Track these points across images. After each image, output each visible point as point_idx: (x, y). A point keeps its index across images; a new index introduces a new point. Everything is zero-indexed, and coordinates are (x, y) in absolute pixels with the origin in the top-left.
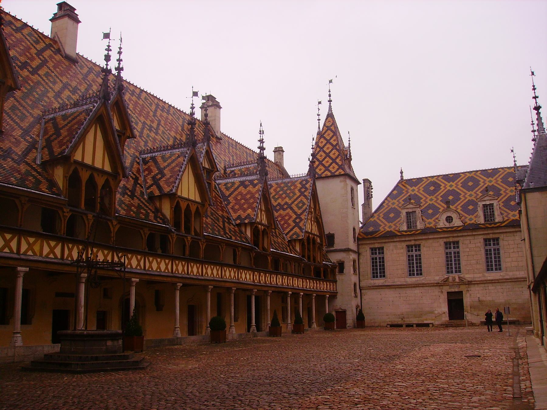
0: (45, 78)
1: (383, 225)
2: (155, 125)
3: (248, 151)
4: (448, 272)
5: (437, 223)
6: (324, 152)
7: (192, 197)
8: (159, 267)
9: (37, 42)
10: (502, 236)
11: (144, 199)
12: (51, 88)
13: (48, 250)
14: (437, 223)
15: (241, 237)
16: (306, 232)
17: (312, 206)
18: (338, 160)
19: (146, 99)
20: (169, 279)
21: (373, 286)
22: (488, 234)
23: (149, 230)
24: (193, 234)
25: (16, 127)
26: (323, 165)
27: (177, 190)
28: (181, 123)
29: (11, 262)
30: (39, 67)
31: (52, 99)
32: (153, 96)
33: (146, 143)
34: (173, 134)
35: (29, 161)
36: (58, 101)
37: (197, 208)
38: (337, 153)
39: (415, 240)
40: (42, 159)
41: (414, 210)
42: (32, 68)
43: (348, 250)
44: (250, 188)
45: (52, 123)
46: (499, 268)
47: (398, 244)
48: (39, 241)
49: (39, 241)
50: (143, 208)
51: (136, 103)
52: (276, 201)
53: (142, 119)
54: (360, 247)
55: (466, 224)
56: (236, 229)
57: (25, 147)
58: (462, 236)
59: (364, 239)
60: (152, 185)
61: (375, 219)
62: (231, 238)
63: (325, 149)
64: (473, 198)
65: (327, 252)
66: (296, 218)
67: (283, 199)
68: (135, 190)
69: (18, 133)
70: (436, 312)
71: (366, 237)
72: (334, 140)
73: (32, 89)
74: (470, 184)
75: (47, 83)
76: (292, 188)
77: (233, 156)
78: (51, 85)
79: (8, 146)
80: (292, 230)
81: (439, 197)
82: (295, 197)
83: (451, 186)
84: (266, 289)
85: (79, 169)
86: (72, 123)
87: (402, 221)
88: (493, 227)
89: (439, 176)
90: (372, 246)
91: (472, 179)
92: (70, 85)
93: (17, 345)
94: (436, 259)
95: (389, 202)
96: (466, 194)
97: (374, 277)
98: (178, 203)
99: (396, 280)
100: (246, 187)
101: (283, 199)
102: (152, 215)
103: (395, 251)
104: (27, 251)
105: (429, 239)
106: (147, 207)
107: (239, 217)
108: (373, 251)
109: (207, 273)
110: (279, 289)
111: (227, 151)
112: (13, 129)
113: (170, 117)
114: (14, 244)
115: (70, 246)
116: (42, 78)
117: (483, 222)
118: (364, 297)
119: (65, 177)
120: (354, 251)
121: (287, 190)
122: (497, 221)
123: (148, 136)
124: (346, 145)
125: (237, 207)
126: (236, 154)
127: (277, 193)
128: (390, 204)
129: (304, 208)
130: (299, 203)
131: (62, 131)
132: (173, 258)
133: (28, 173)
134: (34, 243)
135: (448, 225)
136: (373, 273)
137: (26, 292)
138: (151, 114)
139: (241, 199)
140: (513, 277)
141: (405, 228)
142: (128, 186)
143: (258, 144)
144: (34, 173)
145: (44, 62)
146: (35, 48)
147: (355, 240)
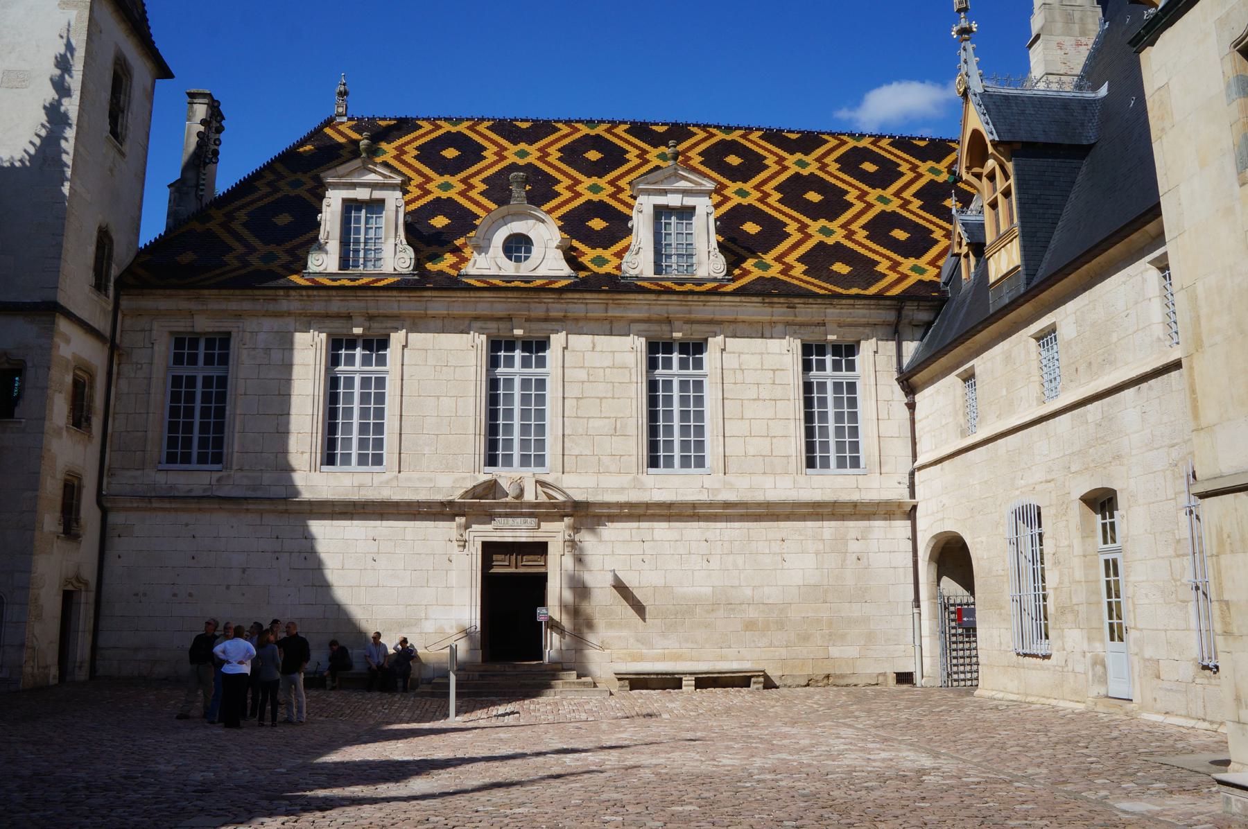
1: (240, 249)
4: (492, 461)
14: (465, 260)
21: (161, 498)
41: (378, 194)
46: (694, 458)
55: (582, 274)
70: (429, 627)
81: (475, 181)
83: (522, 154)
88: (692, 293)
90: (181, 326)
91: (597, 142)
95: (281, 177)
97: (171, 459)
108: (184, 346)
117: (649, 272)
118: (119, 546)
122: (701, 273)
128: (282, 184)
135: (509, 268)
136: (172, 442)
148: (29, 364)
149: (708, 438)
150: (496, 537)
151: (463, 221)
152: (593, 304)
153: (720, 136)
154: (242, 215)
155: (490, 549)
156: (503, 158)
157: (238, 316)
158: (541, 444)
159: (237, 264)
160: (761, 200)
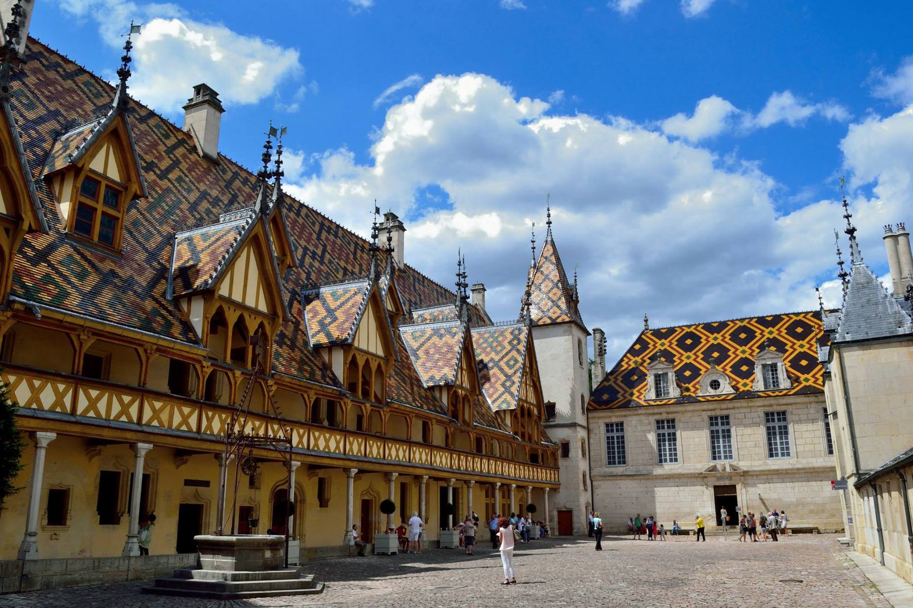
0: (176, 184)
1: (622, 392)
2: (319, 252)
3: (439, 289)
4: (714, 458)
5: (697, 389)
7: (372, 350)
8: (327, 446)
9: (167, 137)
10: (789, 409)
11: (308, 351)
12: (184, 197)
13: (180, 418)
15: (434, 406)
16: (520, 400)
17: (528, 364)
18: (560, 303)
19: (307, 216)
20: (340, 463)
22: (771, 406)
23: (316, 394)
24: (373, 400)
25: (139, 248)
27: (353, 339)
28: (352, 250)
29: (129, 435)
30: (169, 170)
31: (187, 213)
32: (316, 212)
33: (308, 274)
34: (343, 264)
35: (157, 296)
36: (193, 216)
37: (379, 366)
39: (668, 413)
40: (174, 292)
41: (665, 371)
42: (160, 169)
43: (574, 425)
44: (447, 338)
45: (189, 245)
47: (643, 418)
48: (169, 407)
49: (169, 407)
50: (307, 364)
51: (294, 222)
53: (303, 243)
54: (590, 421)
56: (428, 393)
57: (151, 276)
58: (734, 408)
59: (595, 409)
60: (319, 332)
61: (611, 383)
62: (422, 407)
64: (746, 355)
67: (488, 354)
68: (296, 338)
69: (141, 257)
73: (161, 198)
74: (743, 336)
75: (179, 191)
76: (500, 339)
77: (420, 295)
78: (185, 193)
79: (129, 274)
80: (500, 397)
81: (699, 354)
82: (504, 352)
83: (716, 339)
84: (467, 478)
85: (225, 307)
86: (216, 245)
87: (648, 386)
89: (699, 324)
90: (608, 421)
92: (209, 195)
93: (132, 554)
94: (697, 440)
95: (630, 360)
96: (737, 350)
97: (610, 463)
98: (354, 357)
99: (641, 468)
100: (441, 336)
102: (319, 373)
103: (639, 428)
104: (151, 420)
105: (686, 411)
106: (312, 362)
107: (432, 378)
109: (390, 454)
110: (485, 479)
111: (412, 288)
112: (136, 252)
113: (339, 241)
114: (134, 411)
115: (210, 414)
116: (172, 184)
118: (597, 492)
119: (205, 317)
120: (583, 427)
122: (782, 387)
123: (311, 266)
124: (571, 281)
125: (429, 364)
126: (424, 291)
130: (509, 361)
131: (202, 256)
132: (346, 432)
133: (156, 312)
134: (162, 409)
136: (609, 458)
137: (146, 478)
138: (314, 236)
139: (434, 354)
140: (806, 466)
141: (652, 395)
142: (287, 333)
143: (456, 279)
144: (164, 312)
145: (176, 164)
146: (164, 143)
147: (583, 412)
149: (790, 446)
150: (718, 484)
151: (696, 372)
152: (743, 403)
153: (795, 318)
154: (620, 378)
155: (716, 487)
156: (708, 342)
157: (625, 416)
158: (730, 452)
159: (622, 398)
160: (809, 349)
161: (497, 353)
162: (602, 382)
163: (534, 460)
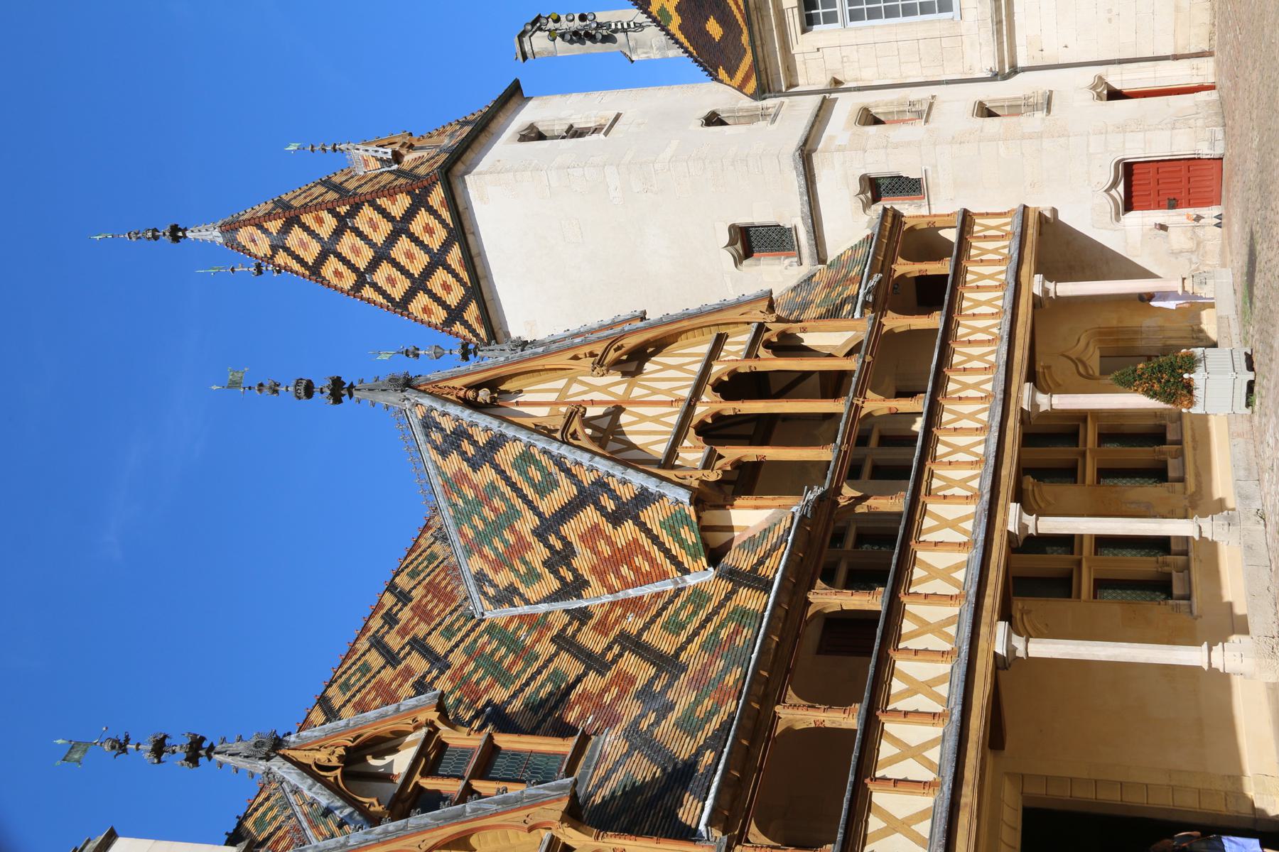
6: (374, 265)
26: (428, 272)
38: (367, 211)
52: (539, 577)
63: (362, 264)
65: (821, 258)
66: (601, 509)
67: (522, 545)
71: (748, 60)
72: (320, 221)
80: (655, 539)
82: (507, 491)
90: (794, 20)
101: (522, 545)
121: (484, 520)
127: (500, 563)
129: (545, 460)
130: (530, 481)
148: (863, 172)
161: (514, 514)
162: (672, 37)
163: (933, 294)
